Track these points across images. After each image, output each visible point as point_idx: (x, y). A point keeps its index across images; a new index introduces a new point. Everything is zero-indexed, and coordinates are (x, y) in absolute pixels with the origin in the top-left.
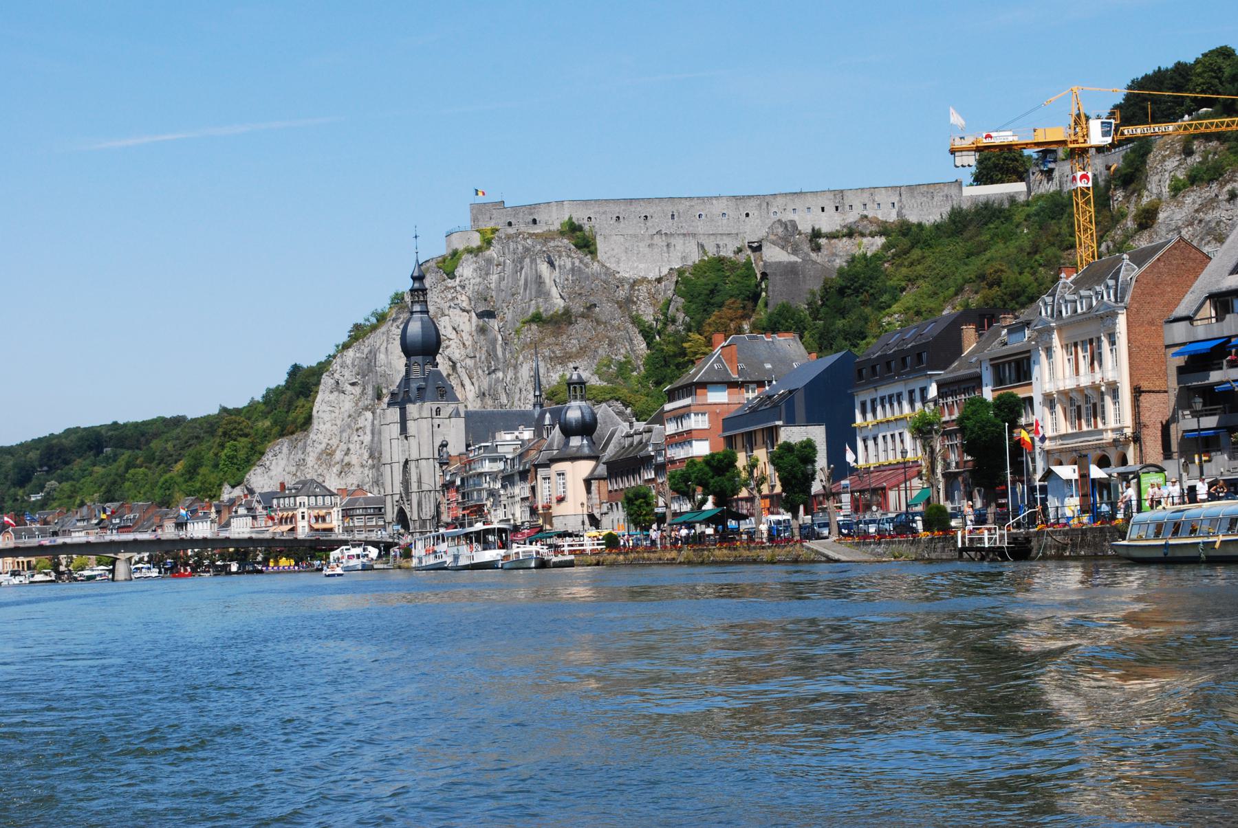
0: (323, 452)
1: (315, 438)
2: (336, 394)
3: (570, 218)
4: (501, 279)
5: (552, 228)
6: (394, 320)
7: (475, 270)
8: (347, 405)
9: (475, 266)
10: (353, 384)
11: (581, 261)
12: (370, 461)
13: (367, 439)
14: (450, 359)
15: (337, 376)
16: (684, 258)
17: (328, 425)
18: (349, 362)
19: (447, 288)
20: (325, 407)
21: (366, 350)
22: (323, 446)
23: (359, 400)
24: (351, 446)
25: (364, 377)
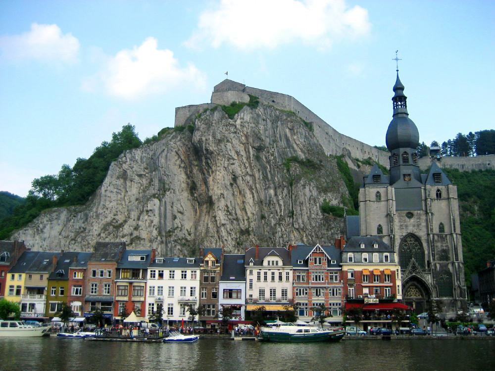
1: (100, 211)
4: (266, 130)
6: (173, 138)
8: (134, 190)
11: (309, 134)
12: (159, 238)
13: (156, 220)
15: (125, 166)
16: (332, 151)
17: (114, 204)
20: (111, 188)
21: (151, 153)
22: (109, 219)
23: (147, 188)
24: (140, 223)
25: (151, 172)
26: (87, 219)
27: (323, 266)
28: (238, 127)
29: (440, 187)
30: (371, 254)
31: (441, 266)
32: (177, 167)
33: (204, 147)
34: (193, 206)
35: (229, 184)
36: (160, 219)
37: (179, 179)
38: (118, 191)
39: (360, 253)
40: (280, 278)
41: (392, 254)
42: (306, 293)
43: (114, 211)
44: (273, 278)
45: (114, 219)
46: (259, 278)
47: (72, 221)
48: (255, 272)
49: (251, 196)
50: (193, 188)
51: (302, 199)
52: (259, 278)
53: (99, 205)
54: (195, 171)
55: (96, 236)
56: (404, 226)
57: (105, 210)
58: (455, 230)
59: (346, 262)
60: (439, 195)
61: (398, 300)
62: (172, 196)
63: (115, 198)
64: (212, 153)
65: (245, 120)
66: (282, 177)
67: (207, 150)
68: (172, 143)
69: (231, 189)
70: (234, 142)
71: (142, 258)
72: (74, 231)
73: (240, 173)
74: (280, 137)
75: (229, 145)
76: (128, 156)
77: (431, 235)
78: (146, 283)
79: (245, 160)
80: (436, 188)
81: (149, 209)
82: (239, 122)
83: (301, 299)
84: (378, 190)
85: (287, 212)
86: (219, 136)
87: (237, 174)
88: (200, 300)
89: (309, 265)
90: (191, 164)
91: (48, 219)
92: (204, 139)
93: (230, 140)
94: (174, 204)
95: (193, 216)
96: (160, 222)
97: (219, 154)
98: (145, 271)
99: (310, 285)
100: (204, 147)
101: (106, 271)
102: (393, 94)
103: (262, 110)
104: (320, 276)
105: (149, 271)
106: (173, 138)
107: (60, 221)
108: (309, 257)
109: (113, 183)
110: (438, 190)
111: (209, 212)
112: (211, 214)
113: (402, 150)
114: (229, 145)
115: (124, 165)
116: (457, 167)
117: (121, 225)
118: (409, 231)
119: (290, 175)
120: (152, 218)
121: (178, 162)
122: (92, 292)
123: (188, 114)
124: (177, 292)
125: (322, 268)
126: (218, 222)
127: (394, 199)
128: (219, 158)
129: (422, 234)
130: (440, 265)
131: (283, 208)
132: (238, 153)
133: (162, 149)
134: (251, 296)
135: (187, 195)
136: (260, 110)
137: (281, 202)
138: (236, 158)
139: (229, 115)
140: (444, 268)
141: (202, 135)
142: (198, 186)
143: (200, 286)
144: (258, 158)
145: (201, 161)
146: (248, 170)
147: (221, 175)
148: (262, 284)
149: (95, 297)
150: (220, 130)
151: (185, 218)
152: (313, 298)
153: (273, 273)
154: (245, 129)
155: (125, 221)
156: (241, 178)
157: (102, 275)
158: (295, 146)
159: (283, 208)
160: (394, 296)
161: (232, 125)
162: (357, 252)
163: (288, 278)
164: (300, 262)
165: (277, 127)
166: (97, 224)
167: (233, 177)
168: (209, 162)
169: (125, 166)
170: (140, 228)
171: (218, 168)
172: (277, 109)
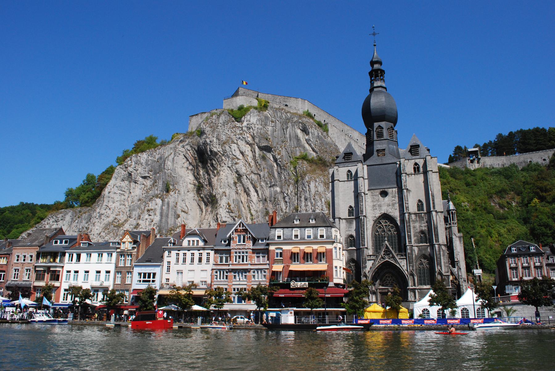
0: (109, 224)
1: (103, 211)
2: (127, 182)
3: (308, 111)
5: (299, 112)
6: (181, 141)
7: (259, 120)
8: (137, 191)
9: (259, 118)
10: (145, 178)
11: (322, 134)
14: (237, 172)
15: (130, 169)
17: (117, 204)
18: (143, 161)
19: (235, 126)
20: (115, 190)
21: (157, 157)
22: (111, 219)
23: (150, 189)
24: (140, 222)
25: (155, 173)
26: (91, 219)
27: (247, 244)
29: (417, 161)
30: (303, 229)
31: (419, 250)
32: (185, 169)
33: (208, 149)
35: (232, 182)
36: (161, 218)
37: (186, 178)
38: (121, 192)
39: (291, 229)
40: (200, 260)
41: (329, 228)
42: (227, 276)
43: (116, 211)
44: (192, 260)
45: (116, 219)
46: (178, 260)
47: (76, 221)
48: (174, 253)
49: (256, 194)
50: (199, 188)
52: (178, 260)
55: (96, 235)
56: (377, 206)
57: (107, 210)
58: (434, 207)
59: (274, 239)
60: (416, 169)
61: (335, 284)
62: (176, 197)
63: (118, 199)
64: (216, 154)
65: (251, 122)
67: (211, 151)
68: (180, 147)
69: (234, 188)
70: (239, 143)
71: (66, 242)
72: (77, 231)
73: (245, 171)
74: (290, 135)
75: (234, 146)
76: (134, 159)
77: (407, 215)
78: (63, 267)
79: (250, 160)
80: (413, 162)
81: (150, 208)
82: (245, 124)
83: (221, 283)
84: (349, 168)
85: (292, 208)
86: (224, 138)
87: (241, 173)
88: (114, 284)
89: (232, 244)
90: (197, 165)
91: (53, 220)
92: (208, 141)
93: (236, 141)
94: (178, 203)
95: (198, 216)
96: (161, 220)
97: (223, 155)
98: (64, 254)
99: (231, 267)
100: (208, 149)
101: (28, 256)
102: (370, 69)
103: (271, 112)
104: (243, 256)
105: (67, 255)
107: (65, 222)
108: (230, 235)
109: (117, 185)
110: (416, 164)
113: (376, 125)
114: (234, 146)
115: (129, 168)
117: (123, 224)
118: (383, 212)
119: (296, 172)
120: (152, 217)
122: (14, 278)
124: (92, 275)
125: (246, 247)
126: (219, 220)
127: (366, 177)
128: (223, 158)
129: (396, 214)
130: (419, 249)
133: (169, 153)
134: (168, 280)
135: (193, 195)
138: (240, 157)
139: (235, 119)
140: (423, 252)
143: (115, 269)
145: (207, 163)
146: (254, 168)
147: (224, 174)
148: (180, 267)
149: (16, 283)
150: (225, 132)
151: (189, 217)
152: (234, 283)
153: (193, 254)
154: (251, 130)
155: (126, 221)
156: (245, 177)
157: (24, 260)
160: (330, 278)
161: (239, 127)
162: (288, 228)
163: (208, 260)
164: (225, 242)
165: (287, 128)
166: (99, 224)
167: (237, 176)
168: (214, 162)
169: (130, 169)
170: (140, 227)
171: (222, 168)
172: (288, 112)
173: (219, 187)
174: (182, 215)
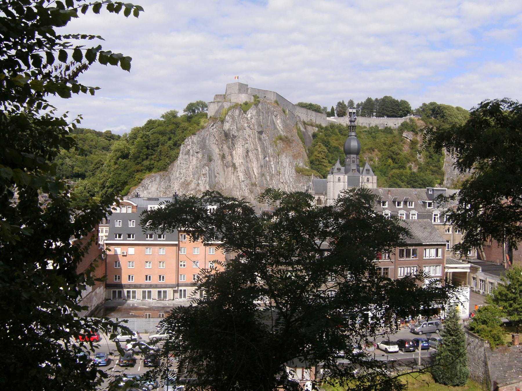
4: (263, 119)
6: (212, 126)
13: (208, 179)
15: (189, 147)
22: (183, 180)
24: (200, 182)
28: (249, 119)
29: (369, 177)
34: (223, 168)
50: (223, 157)
51: (284, 165)
53: (177, 172)
54: (225, 147)
60: (368, 180)
64: (236, 137)
66: (274, 150)
67: (233, 135)
76: (190, 140)
80: (367, 177)
82: (249, 116)
92: (231, 128)
106: (212, 126)
111: (234, 173)
112: (235, 174)
116: (365, 125)
121: (215, 141)
123: (217, 108)
131: (273, 169)
132: (249, 136)
136: (260, 106)
137: (273, 166)
141: (231, 126)
142: (226, 156)
144: (260, 139)
158: (278, 127)
159: (273, 169)
169: (189, 147)
173: (238, 159)
174: (217, 175)
